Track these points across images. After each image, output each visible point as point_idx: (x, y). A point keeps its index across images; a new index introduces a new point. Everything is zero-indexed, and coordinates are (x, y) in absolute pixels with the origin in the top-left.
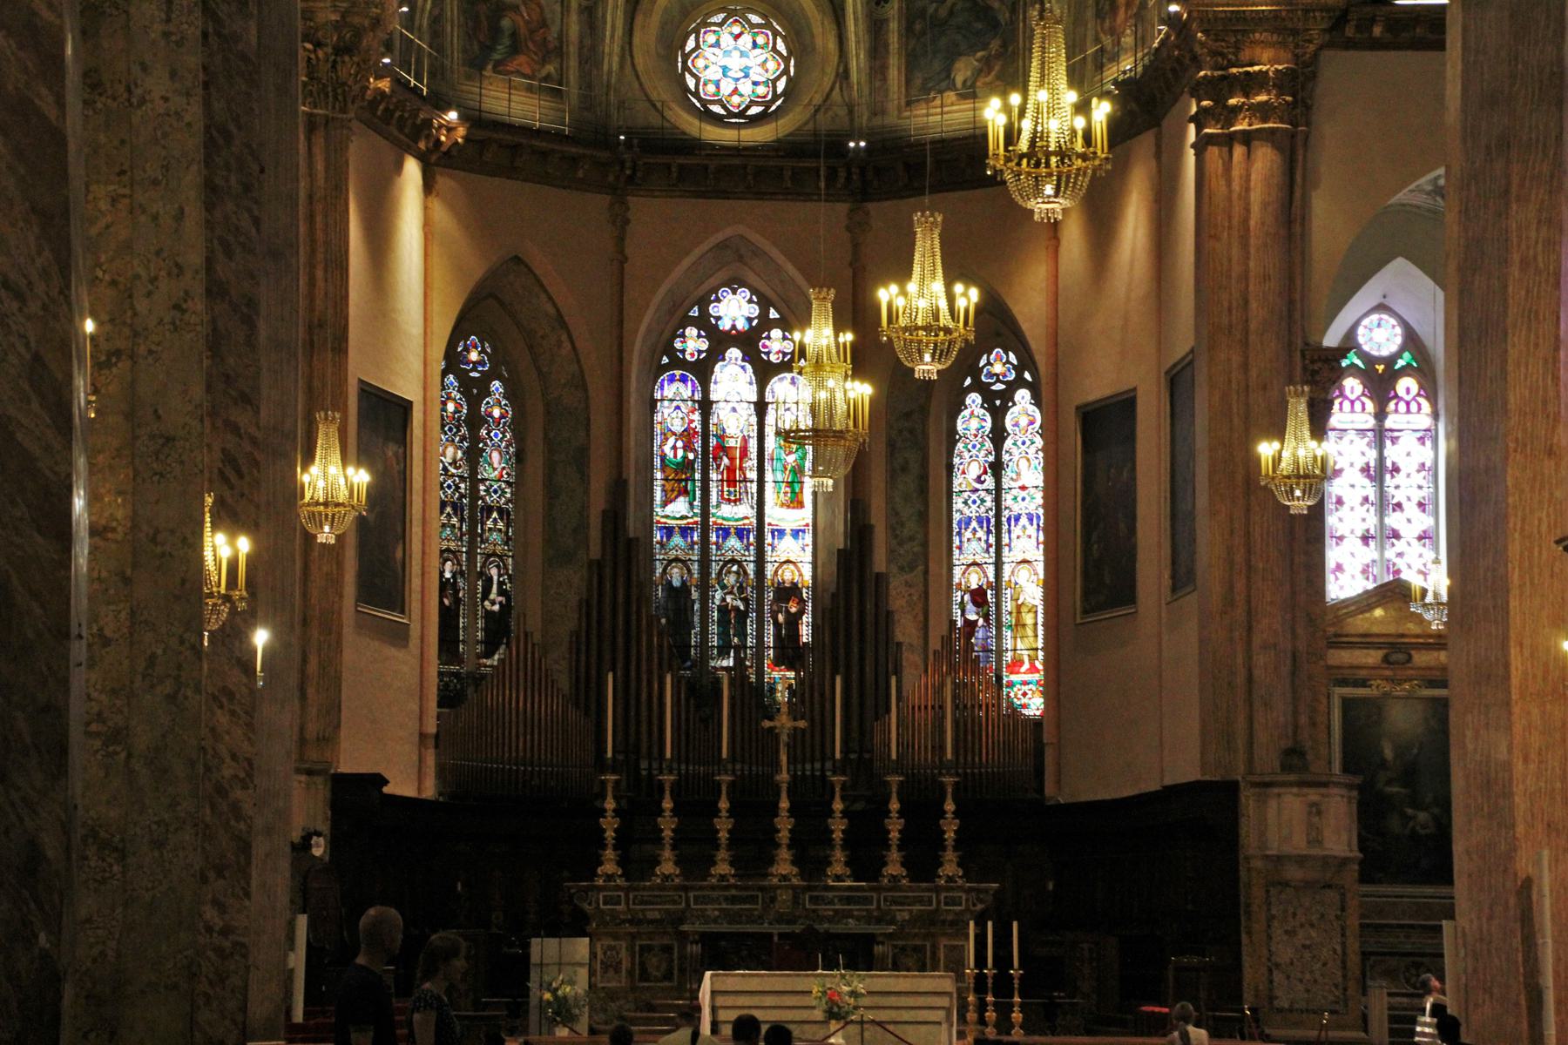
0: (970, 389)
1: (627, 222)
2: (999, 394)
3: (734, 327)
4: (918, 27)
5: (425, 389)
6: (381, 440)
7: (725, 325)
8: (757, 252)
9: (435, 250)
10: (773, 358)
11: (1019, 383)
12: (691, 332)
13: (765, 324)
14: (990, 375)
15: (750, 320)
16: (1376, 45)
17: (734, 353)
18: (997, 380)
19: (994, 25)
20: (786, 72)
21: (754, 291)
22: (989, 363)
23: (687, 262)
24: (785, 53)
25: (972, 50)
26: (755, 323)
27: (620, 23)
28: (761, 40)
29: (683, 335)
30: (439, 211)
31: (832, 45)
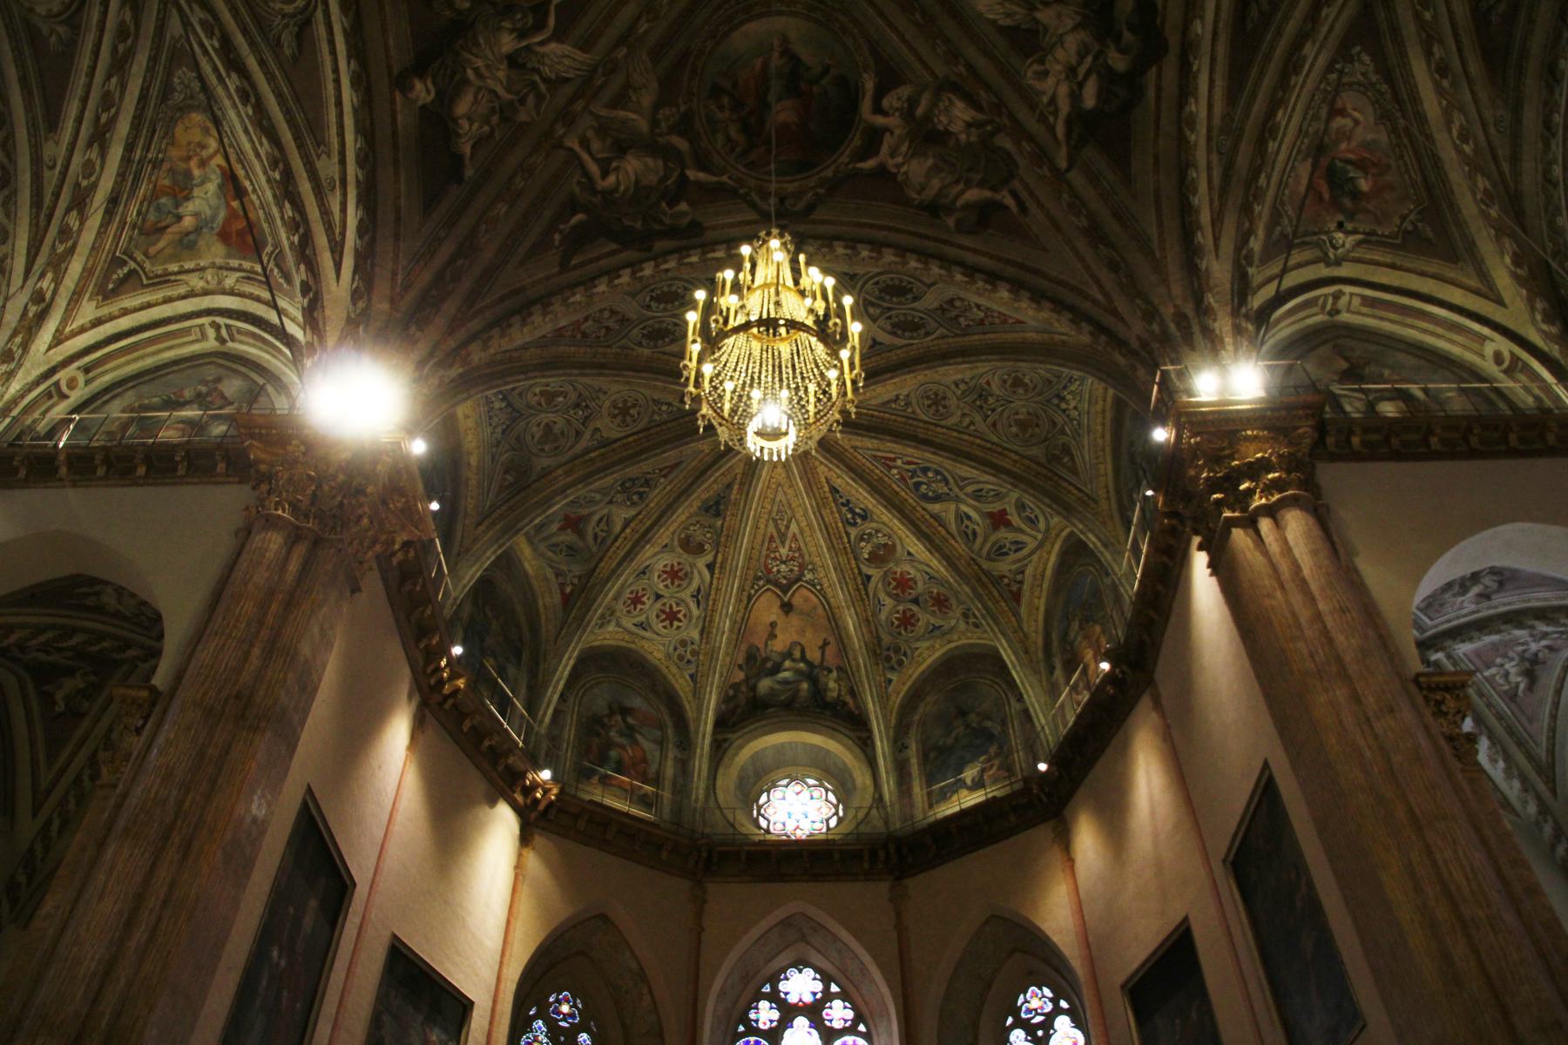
0: (1013, 1027)
1: (705, 902)
2: (1040, 1026)
3: (801, 1000)
4: (932, 755)
5: (495, 1002)
6: (420, 1018)
7: (793, 999)
8: (819, 927)
9: (525, 891)
10: (837, 1025)
11: (1057, 1011)
12: (764, 1005)
13: (828, 997)
14: (1029, 1011)
15: (814, 994)
16: (1357, 457)
17: (801, 1022)
18: (1037, 1014)
19: (990, 737)
20: (836, 813)
21: (816, 970)
22: (1026, 1001)
23: (755, 932)
24: (835, 801)
25: (974, 758)
26: (819, 996)
27: (705, 767)
28: (816, 794)
29: (757, 1008)
30: (532, 861)
31: (869, 781)
